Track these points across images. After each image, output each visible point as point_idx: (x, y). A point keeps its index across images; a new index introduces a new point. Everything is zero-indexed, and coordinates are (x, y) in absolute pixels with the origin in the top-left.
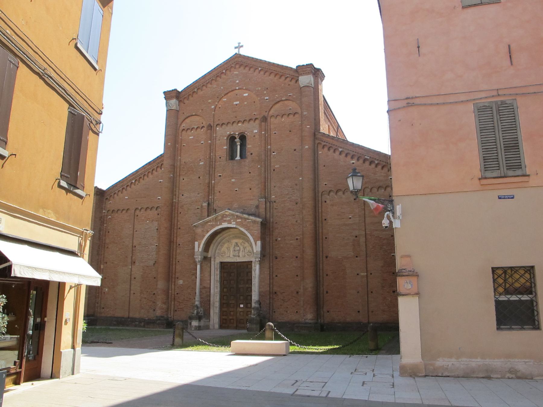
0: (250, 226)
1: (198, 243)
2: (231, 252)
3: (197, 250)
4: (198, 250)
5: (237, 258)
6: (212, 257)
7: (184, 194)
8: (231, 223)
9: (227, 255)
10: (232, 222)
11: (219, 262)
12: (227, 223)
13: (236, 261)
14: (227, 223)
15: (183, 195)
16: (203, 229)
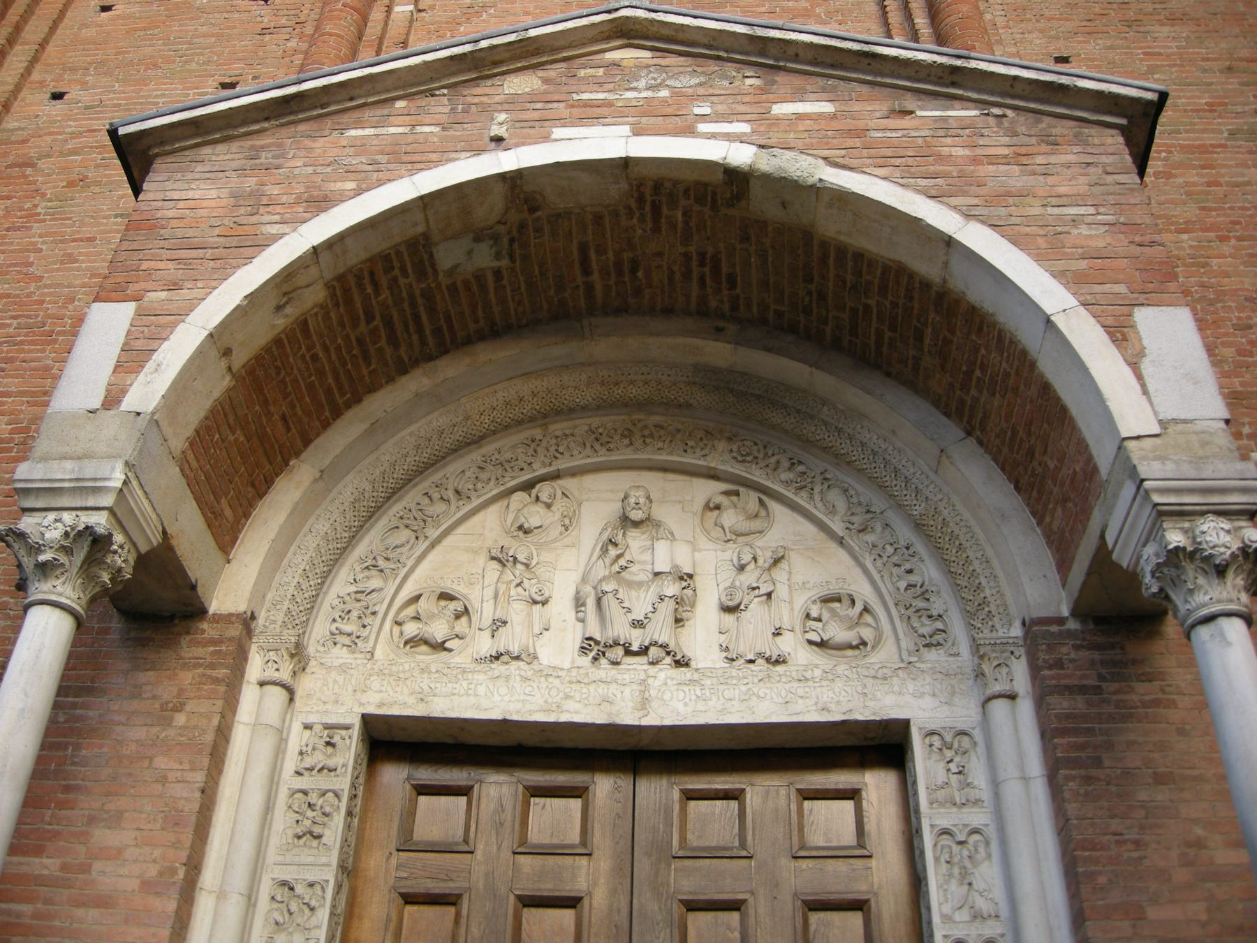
0: (975, 161)
1: (139, 313)
2: (561, 606)
3: (96, 403)
4: (112, 400)
5: (665, 673)
6: (261, 621)
7: (74, 93)
8: (690, 131)
9: (485, 645)
10: (703, 118)
11: (350, 713)
12: (626, 129)
13: (629, 718)
14: (626, 129)
15: (57, 96)
16: (251, 182)
